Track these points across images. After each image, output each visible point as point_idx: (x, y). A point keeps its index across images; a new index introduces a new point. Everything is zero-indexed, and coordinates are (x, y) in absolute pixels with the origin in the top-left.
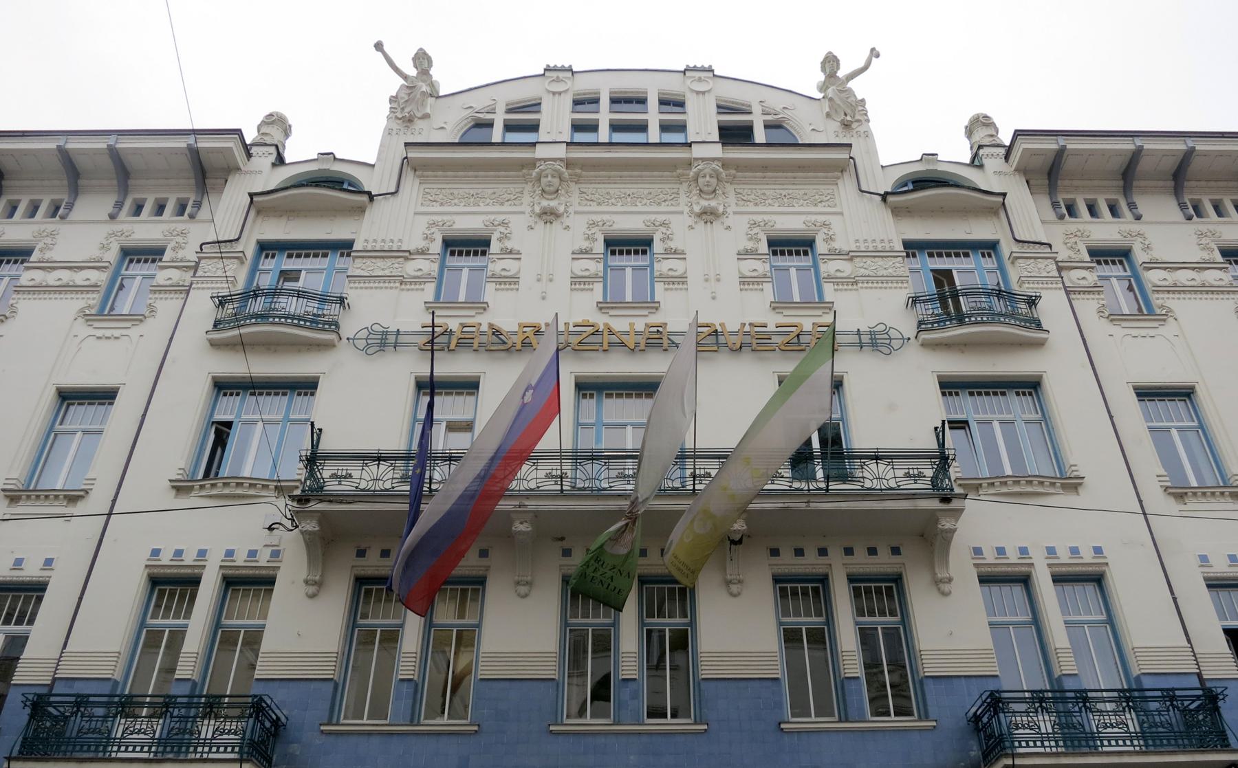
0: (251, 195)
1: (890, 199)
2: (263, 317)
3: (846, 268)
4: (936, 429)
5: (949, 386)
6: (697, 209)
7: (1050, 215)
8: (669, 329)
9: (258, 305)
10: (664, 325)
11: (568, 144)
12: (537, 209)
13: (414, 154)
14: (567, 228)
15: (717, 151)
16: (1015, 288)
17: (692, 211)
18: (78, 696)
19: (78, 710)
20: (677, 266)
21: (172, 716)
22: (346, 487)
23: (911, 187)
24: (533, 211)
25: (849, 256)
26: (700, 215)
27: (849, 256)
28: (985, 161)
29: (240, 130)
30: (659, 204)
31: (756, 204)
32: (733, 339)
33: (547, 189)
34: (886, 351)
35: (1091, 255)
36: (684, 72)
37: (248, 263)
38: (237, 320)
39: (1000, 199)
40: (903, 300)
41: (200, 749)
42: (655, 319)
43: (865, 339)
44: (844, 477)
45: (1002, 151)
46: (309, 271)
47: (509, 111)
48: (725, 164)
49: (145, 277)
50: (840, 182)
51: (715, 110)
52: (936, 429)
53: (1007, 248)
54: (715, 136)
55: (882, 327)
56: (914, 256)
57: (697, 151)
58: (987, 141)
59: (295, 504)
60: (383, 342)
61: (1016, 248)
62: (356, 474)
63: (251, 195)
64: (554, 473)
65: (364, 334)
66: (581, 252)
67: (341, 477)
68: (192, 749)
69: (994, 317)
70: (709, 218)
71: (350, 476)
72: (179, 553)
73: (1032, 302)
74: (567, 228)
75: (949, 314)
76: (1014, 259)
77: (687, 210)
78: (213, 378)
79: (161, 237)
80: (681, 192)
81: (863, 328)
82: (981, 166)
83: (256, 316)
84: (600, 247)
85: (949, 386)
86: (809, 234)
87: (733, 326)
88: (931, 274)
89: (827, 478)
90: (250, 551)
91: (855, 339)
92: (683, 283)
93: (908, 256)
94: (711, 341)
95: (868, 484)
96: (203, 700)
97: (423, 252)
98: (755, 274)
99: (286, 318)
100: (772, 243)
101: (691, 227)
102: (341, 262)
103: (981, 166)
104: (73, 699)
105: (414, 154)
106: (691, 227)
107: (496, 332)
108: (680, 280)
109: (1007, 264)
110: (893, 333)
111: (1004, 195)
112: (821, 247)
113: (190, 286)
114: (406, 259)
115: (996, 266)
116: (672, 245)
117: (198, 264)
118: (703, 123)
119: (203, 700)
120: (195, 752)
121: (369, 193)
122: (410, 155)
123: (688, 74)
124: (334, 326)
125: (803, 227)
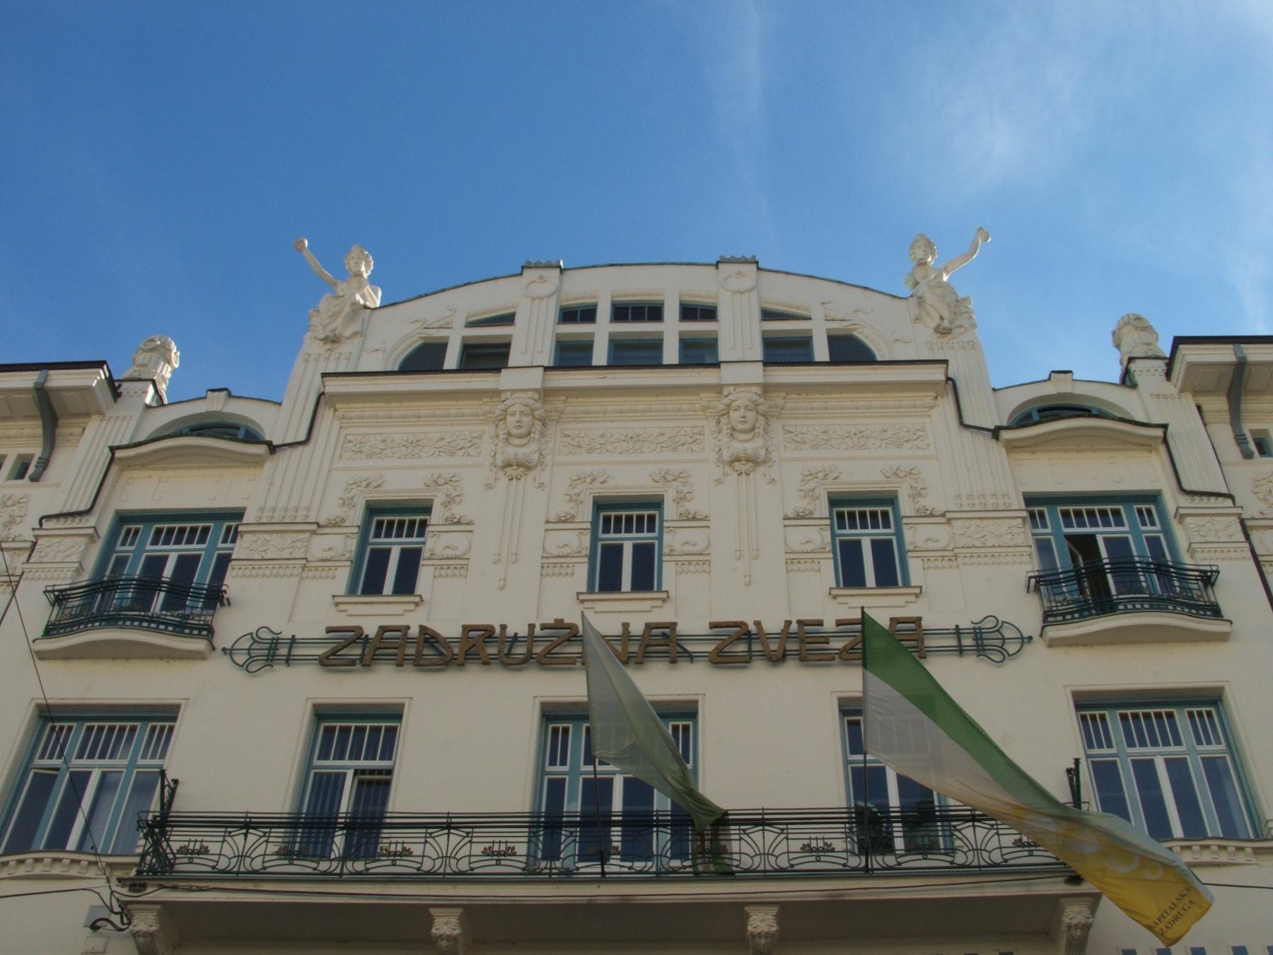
0: (113, 449)
1: (1005, 435)
3: (938, 534)
4: (1069, 771)
5: (1091, 707)
6: (726, 455)
7: (1230, 450)
10: (673, 626)
11: (546, 369)
12: (499, 461)
13: (334, 386)
14: (541, 485)
15: (756, 373)
16: (1187, 560)
17: (720, 460)
22: (201, 865)
23: (1036, 417)
24: (494, 465)
25: (946, 518)
26: (731, 463)
27: (946, 518)
28: (1139, 379)
29: (105, 362)
30: (675, 449)
31: (815, 447)
32: (774, 646)
33: (515, 431)
34: (998, 658)
36: (717, 265)
39: (1159, 432)
40: (1023, 581)
42: (662, 615)
43: (968, 641)
44: (928, 849)
45: (1161, 365)
47: (471, 325)
48: (767, 389)
50: (933, 413)
51: (757, 315)
52: (1069, 771)
53: (1172, 500)
54: (757, 352)
55: (989, 624)
57: (727, 374)
58: (1139, 352)
59: (125, 891)
60: (272, 652)
61: (1184, 501)
62: (214, 848)
63: (113, 449)
64: (496, 848)
65: (246, 644)
66: (560, 521)
67: (193, 852)
69: (1157, 604)
71: (205, 851)
74: (541, 485)
75: (1086, 601)
76: (1181, 518)
77: (714, 456)
80: (707, 432)
81: (965, 624)
82: (1134, 386)
84: (586, 513)
86: (887, 487)
87: (773, 625)
88: (1066, 543)
89: (909, 850)
91: (952, 642)
92: (704, 562)
93: (1032, 515)
94: (737, 646)
95: (960, 858)
97: (337, 524)
98: (810, 547)
99: (159, 623)
100: (834, 501)
101: (718, 481)
103: (1134, 386)
105: (334, 386)
106: (718, 481)
107: (429, 637)
108: (701, 558)
109: (1175, 525)
110: (1008, 633)
111: (1165, 427)
112: (906, 506)
113: (21, 576)
114: (314, 533)
117: (35, 544)
118: (739, 335)
121: (269, 444)
122: (329, 389)
123: (720, 266)
124: (208, 631)
125: (881, 478)
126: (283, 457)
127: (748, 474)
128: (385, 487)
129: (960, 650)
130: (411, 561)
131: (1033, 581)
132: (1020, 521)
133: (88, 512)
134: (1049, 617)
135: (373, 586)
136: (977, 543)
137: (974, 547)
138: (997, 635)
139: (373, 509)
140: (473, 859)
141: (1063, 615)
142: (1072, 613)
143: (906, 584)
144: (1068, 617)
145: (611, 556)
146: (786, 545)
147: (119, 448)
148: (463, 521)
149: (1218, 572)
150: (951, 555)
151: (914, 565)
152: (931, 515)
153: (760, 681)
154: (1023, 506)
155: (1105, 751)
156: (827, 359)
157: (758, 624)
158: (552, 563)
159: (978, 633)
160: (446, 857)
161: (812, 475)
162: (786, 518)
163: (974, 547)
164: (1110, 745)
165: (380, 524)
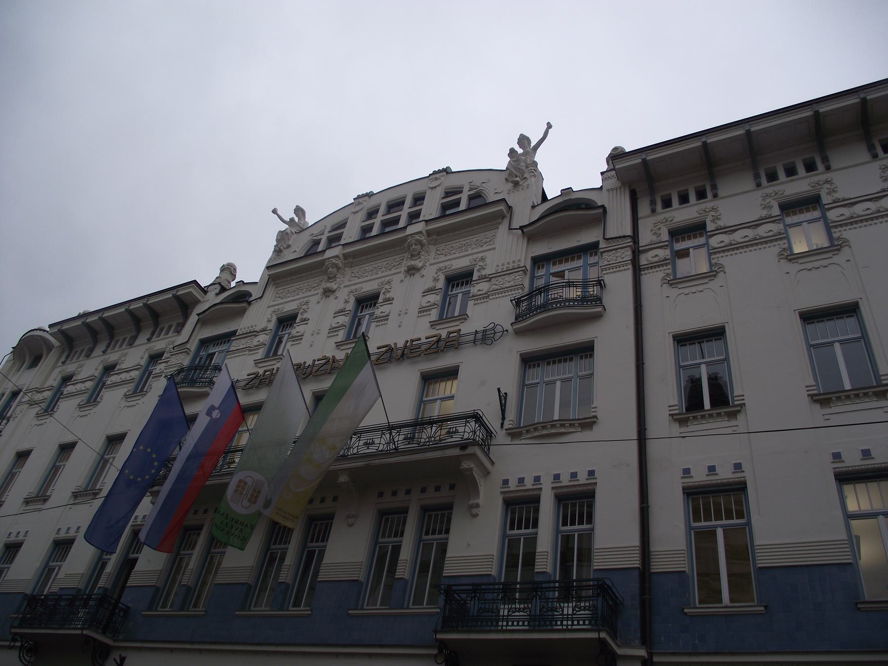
2: (544, 307)
9: (540, 300)
18: (473, 585)
19: (475, 596)
21: (540, 599)
37: (528, 273)
38: (532, 310)
41: (565, 623)
46: (570, 270)
49: (464, 294)
68: (559, 623)
72: (574, 475)
78: (521, 355)
79: (469, 264)
83: (539, 307)
90: (519, 479)
96: (557, 585)
102: (592, 260)
104: (471, 587)
119: (557, 585)
120: (562, 624)
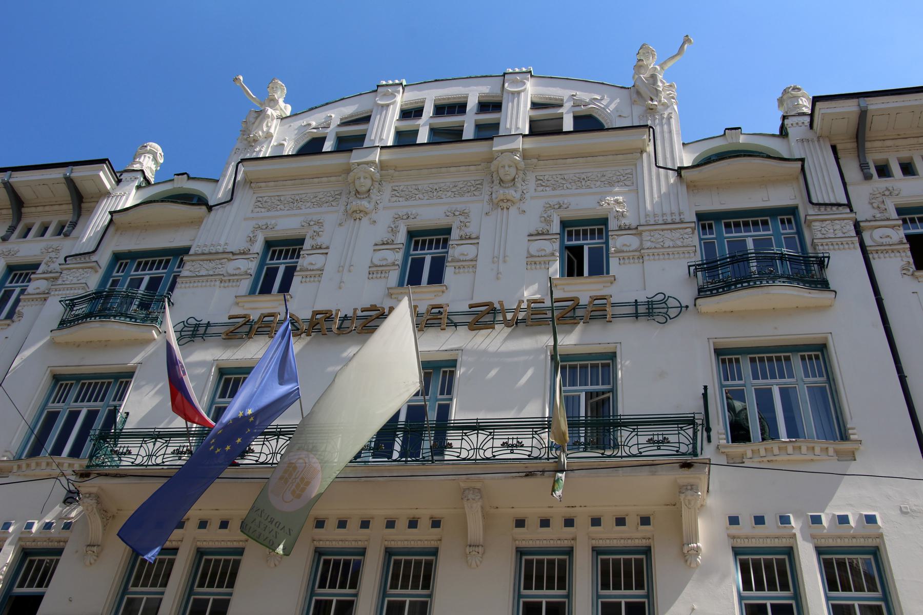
3: (631, 241)
8: (449, 309)
20: (468, 250)
34: (663, 320)
35: (899, 214)
56: (710, 226)
70: (505, 205)
73: (822, 263)
85: (726, 357)
110: (672, 302)
115: (794, 231)
116: (468, 231)
126: (217, 213)
127: (508, 209)
128: (277, 228)
129: (636, 315)
130: (290, 273)
131: (692, 269)
132: (690, 230)
133: (94, 252)
134: (702, 292)
135: (266, 289)
136: (658, 246)
137: (655, 248)
138: (664, 305)
139: (269, 244)
140: (495, 450)
141: (711, 290)
142: (723, 288)
143: (608, 273)
144: (721, 290)
145: (418, 264)
146: (528, 251)
147: (115, 212)
148: (324, 246)
149: (829, 257)
150: (640, 255)
151: (613, 263)
152: (629, 229)
153: (494, 341)
154: (695, 219)
155: (737, 382)
156: (527, 132)
157: (501, 303)
158: (376, 270)
159: (650, 304)
160: (477, 449)
161: (552, 207)
162: (530, 235)
163: (655, 248)
164: (740, 378)
165: (274, 252)
